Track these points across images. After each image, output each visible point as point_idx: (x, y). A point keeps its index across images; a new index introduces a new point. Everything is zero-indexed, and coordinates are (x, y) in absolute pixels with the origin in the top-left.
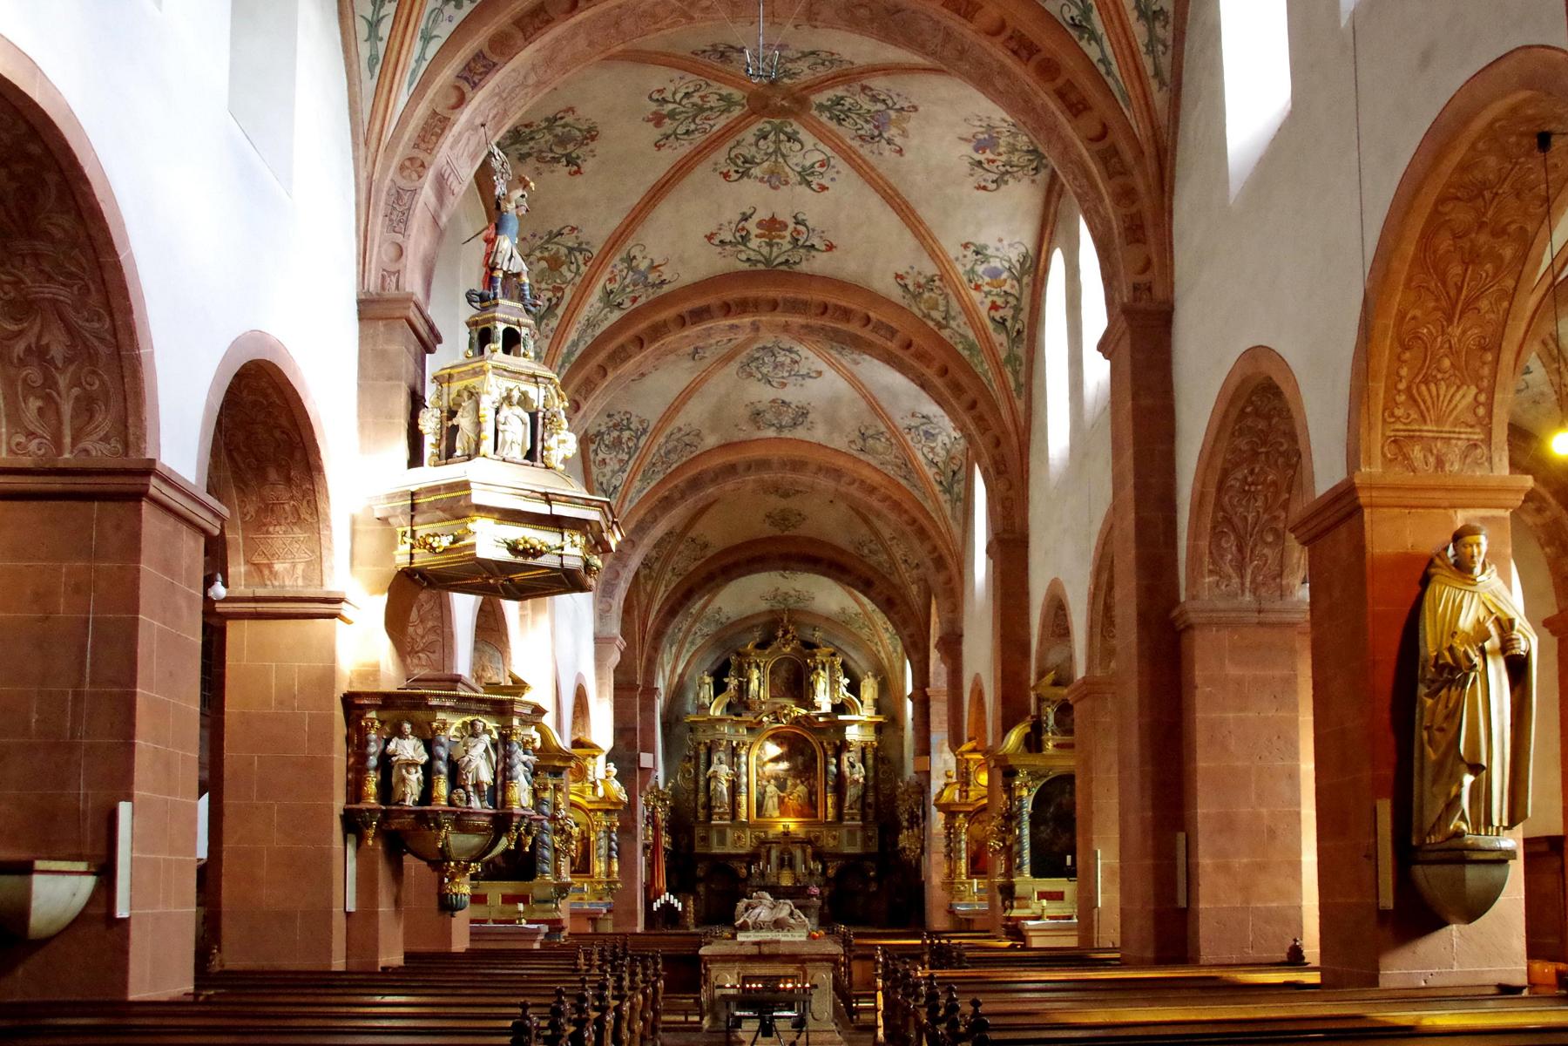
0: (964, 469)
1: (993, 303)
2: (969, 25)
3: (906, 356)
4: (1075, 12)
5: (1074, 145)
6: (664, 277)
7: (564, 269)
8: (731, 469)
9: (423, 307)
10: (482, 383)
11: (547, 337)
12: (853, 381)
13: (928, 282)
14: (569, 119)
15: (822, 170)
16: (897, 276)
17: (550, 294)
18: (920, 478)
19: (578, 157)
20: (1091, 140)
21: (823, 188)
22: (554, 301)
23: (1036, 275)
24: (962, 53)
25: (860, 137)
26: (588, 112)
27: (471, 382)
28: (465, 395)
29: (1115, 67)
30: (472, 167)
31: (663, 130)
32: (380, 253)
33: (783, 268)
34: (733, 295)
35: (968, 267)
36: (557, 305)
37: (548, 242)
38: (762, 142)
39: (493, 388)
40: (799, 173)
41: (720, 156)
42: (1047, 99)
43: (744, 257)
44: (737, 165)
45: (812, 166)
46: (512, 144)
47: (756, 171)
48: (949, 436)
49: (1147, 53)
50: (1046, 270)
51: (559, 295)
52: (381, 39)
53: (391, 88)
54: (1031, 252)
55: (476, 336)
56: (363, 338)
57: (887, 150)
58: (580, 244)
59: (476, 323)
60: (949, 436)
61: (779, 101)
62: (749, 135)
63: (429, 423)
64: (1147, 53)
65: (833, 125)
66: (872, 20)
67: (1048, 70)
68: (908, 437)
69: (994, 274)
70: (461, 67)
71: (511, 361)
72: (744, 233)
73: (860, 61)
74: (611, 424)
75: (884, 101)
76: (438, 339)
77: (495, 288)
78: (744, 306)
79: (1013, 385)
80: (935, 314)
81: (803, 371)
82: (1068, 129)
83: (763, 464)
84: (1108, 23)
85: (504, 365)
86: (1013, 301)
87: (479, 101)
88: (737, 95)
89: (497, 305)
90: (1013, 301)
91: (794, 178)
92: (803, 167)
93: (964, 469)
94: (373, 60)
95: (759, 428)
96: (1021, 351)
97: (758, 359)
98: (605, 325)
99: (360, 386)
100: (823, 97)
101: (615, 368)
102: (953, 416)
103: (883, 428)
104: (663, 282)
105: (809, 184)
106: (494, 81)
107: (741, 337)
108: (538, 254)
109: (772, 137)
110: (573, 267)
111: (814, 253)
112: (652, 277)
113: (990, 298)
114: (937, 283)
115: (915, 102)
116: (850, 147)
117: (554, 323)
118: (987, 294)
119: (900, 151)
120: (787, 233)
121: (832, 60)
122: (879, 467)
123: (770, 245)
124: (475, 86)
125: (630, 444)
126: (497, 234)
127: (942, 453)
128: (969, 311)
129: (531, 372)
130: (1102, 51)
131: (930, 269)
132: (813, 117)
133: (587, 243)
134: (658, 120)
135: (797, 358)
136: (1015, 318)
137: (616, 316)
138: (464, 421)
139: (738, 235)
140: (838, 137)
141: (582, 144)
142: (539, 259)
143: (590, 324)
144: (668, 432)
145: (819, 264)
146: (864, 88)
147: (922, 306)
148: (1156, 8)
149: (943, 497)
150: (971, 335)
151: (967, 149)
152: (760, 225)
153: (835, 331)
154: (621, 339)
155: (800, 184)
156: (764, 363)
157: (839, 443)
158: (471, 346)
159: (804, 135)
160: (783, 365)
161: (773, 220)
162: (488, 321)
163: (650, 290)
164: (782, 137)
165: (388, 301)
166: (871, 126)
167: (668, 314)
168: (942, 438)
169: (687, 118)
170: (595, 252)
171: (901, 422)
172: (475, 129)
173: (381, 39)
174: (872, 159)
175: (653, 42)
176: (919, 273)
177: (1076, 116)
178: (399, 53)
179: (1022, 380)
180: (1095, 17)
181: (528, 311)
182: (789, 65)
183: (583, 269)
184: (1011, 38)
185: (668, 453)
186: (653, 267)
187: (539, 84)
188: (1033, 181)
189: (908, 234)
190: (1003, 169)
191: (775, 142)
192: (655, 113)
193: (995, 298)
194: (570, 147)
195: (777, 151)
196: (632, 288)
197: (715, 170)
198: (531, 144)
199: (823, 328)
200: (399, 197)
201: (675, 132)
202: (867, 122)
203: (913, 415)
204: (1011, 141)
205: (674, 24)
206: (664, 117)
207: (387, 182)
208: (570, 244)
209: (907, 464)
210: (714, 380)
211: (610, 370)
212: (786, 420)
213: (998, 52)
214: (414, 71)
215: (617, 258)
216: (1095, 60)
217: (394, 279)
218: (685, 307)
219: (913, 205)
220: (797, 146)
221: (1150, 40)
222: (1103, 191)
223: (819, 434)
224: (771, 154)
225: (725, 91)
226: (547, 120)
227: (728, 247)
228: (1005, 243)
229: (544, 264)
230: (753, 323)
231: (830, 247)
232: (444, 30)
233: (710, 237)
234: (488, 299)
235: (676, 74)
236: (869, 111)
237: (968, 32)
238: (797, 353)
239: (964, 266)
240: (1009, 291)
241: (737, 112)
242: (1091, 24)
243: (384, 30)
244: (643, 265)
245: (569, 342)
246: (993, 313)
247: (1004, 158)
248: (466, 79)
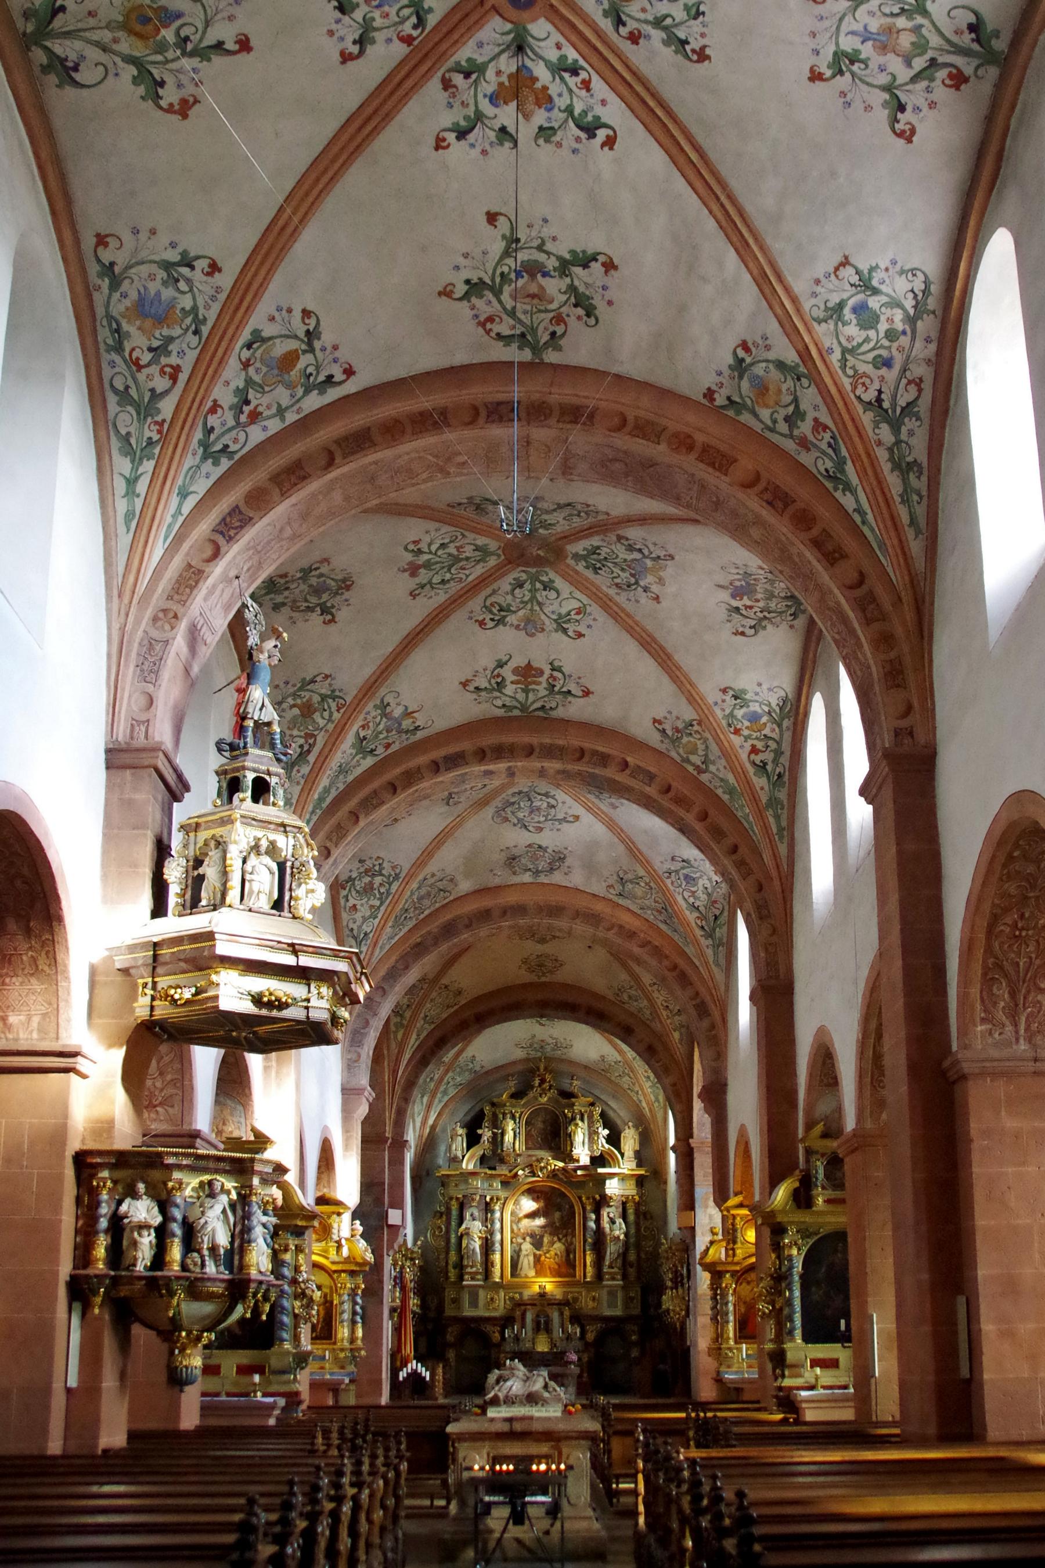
0: (726, 914)
1: (753, 746)
2: (723, 477)
3: (665, 802)
4: (829, 464)
5: (831, 592)
7: (317, 716)
8: (485, 915)
9: (172, 755)
10: (230, 832)
11: (298, 783)
12: (612, 825)
13: (686, 728)
14: (324, 569)
15: (578, 617)
16: (655, 721)
17: (302, 741)
18: (682, 924)
19: (333, 607)
20: (851, 588)
21: (580, 635)
22: (306, 748)
23: (796, 719)
24: (717, 505)
25: (617, 585)
26: (342, 562)
27: (218, 831)
28: (212, 844)
29: (870, 517)
30: (225, 617)
31: (417, 580)
32: (130, 702)
33: (537, 713)
34: (489, 740)
35: (727, 712)
36: (309, 751)
37: (301, 689)
38: (517, 591)
39: (241, 837)
40: (555, 620)
41: (476, 604)
42: (802, 546)
43: (499, 703)
44: (491, 612)
45: (569, 614)
46: (267, 594)
47: (512, 619)
48: (710, 880)
49: (903, 502)
50: (806, 714)
51: (311, 741)
52: (138, 496)
53: (146, 542)
54: (790, 696)
55: (225, 785)
56: (110, 787)
57: (643, 598)
58: (333, 691)
59: (225, 772)
60: (710, 880)
61: (535, 551)
62: (505, 584)
63: (174, 873)
64: (903, 502)
65: (589, 574)
66: (627, 475)
67: (804, 520)
68: (668, 882)
69: (754, 718)
70: (217, 521)
71: (260, 810)
72: (499, 680)
73: (615, 513)
74: (362, 870)
75: (640, 550)
76: (187, 788)
77: (245, 737)
78: (500, 752)
79: (775, 830)
80: (694, 758)
81: (560, 816)
82: (825, 577)
83: (520, 910)
84: (862, 473)
85: (252, 814)
86: (773, 745)
87: (234, 554)
88: (493, 545)
89: (247, 754)
90: (773, 745)
91: (550, 625)
92: (560, 614)
93: (726, 914)
94: (129, 516)
95: (514, 873)
96: (782, 795)
97: (513, 803)
98: (359, 771)
99: (104, 835)
100: (579, 547)
101: (367, 815)
102: (714, 861)
103: (641, 872)
104: (417, 728)
105: (565, 631)
106: (249, 535)
107: (496, 783)
108: (290, 701)
109: (527, 586)
110: (326, 714)
111: (570, 698)
112: (406, 724)
113: (750, 742)
114: (696, 728)
115: (671, 551)
116: (606, 595)
117: (305, 770)
118: (747, 738)
119: (657, 599)
121: (588, 510)
122: (639, 912)
123: (526, 691)
124: (230, 539)
125: (382, 890)
126: (248, 684)
127: (703, 897)
128: (728, 755)
129: (280, 821)
130: (857, 501)
131: (688, 714)
132: (568, 566)
133: (341, 691)
134: (413, 570)
135: (552, 802)
136: (775, 761)
137: (369, 762)
138: (210, 871)
139: (493, 681)
140: (592, 584)
141: (337, 593)
142: (294, 706)
143: (342, 770)
144: (421, 877)
145: (576, 709)
146: (620, 538)
147: (681, 751)
148: (909, 459)
149: (705, 942)
150: (731, 779)
151: (725, 596)
152: (516, 671)
153: (593, 776)
154: (376, 784)
155: (556, 631)
156: (520, 808)
157: (598, 888)
158: (219, 795)
159: (559, 583)
160: (538, 809)
161: (529, 666)
162: (237, 769)
163: (404, 736)
164: (538, 585)
165: (138, 750)
166: (627, 574)
167: (422, 760)
168: (703, 882)
170: (349, 699)
171: (661, 865)
172: (229, 581)
173: (138, 496)
174: (629, 607)
175: (410, 495)
176: (678, 718)
177: (832, 565)
178: (156, 509)
179: (784, 824)
180: (849, 467)
181: (278, 760)
182: (545, 517)
183: (336, 716)
184: (766, 489)
185: (421, 898)
186: (407, 714)
187: (294, 537)
188: (791, 627)
189: (666, 680)
190: (761, 615)
191: (530, 591)
192: (410, 563)
193: (755, 742)
194: (325, 597)
195: (533, 598)
196: (385, 734)
197: (471, 618)
198: (286, 593)
199: (580, 773)
200: (151, 647)
201: (430, 582)
202: (623, 570)
203: (673, 859)
204: (769, 588)
205: (430, 479)
206: (419, 567)
207: (140, 633)
208: (323, 691)
209: (667, 909)
210: (470, 824)
211: (361, 817)
212: (542, 865)
213: (753, 504)
214: (169, 526)
215: (371, 705)
216: (850, 511)
217: (143, 729)
218: (438, 754)
219: (669, 651)
220: (553, 595)
221: (905, 490)
222: (863, 639)
223: (577, 879)
225: (481, 541)
226: (302, 570)
227: (483, 694)
228: (765, 687)
229: (296, 711)
230: (509, 768)
231: (587, 693)
232: (201, 487)
233: (464, 684)
234: (238, 748)
235: (432, 525)
237: (723, 486)
238: (553, 797)
239: (723, 710)
240: (770, 734)
241: (492, 561)
242: (846, 476)
243: (142, 487)
244: (398, 712)
245: (320, 789)
246: (753, 756)
247: (761, 604)
248: (222, 533)
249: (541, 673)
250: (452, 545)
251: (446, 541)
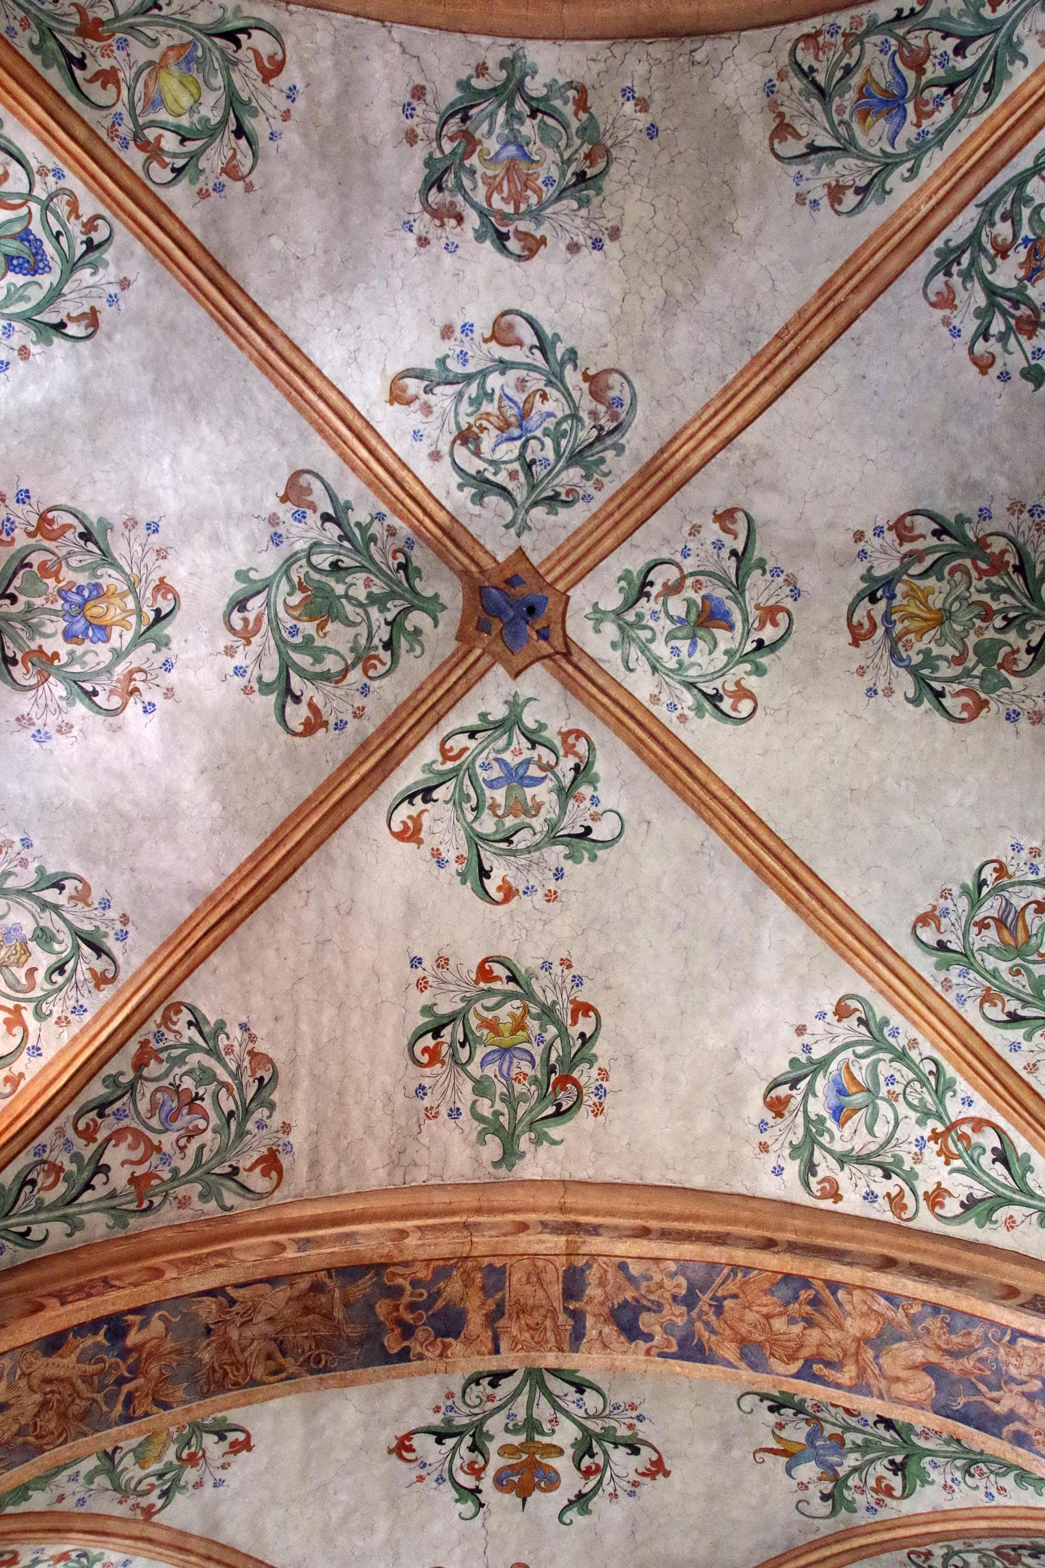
6: (772, 1418)
13: (176, 1480)
43: (592, 1401)
72: (586, 1461)
120: (496, 1462)
123: (532, 1426)
139: (599, 1460)
152: (552, 1482)
196: (849, 1437)
227: (622, 1431)
231: (402, 1447)
233: (658, 1468)
244: (808, 1471)
249: (500, 1482)
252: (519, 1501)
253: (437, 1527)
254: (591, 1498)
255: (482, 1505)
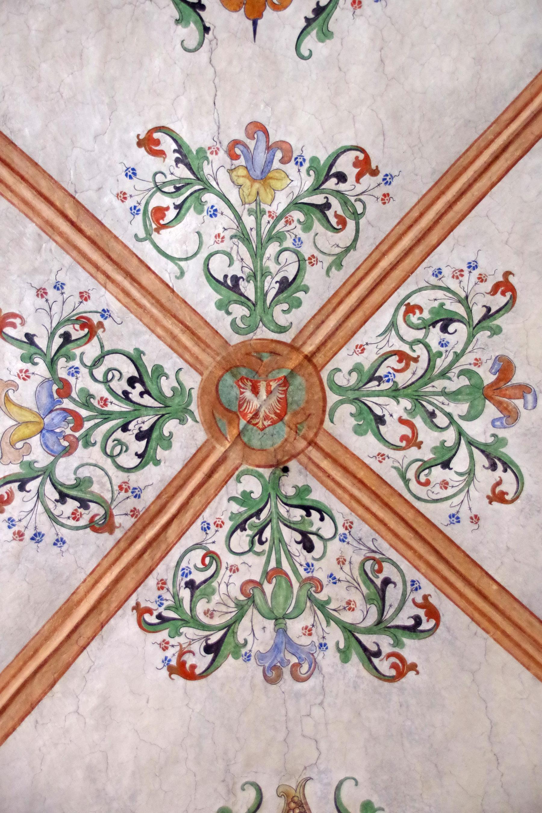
15: (160, 200)
40: (207, 188)
44: (345, 201)
75: (63, 498)
92: (200, 206)
169: (443, 375)
197: (388, 180)
224: (270, 239)
236: (87, 444)
250: (426, 454)
251: (438, 473)
252: (249, 23)
253: (157, 63)
254: (329, 16)
255: (207, 30)
